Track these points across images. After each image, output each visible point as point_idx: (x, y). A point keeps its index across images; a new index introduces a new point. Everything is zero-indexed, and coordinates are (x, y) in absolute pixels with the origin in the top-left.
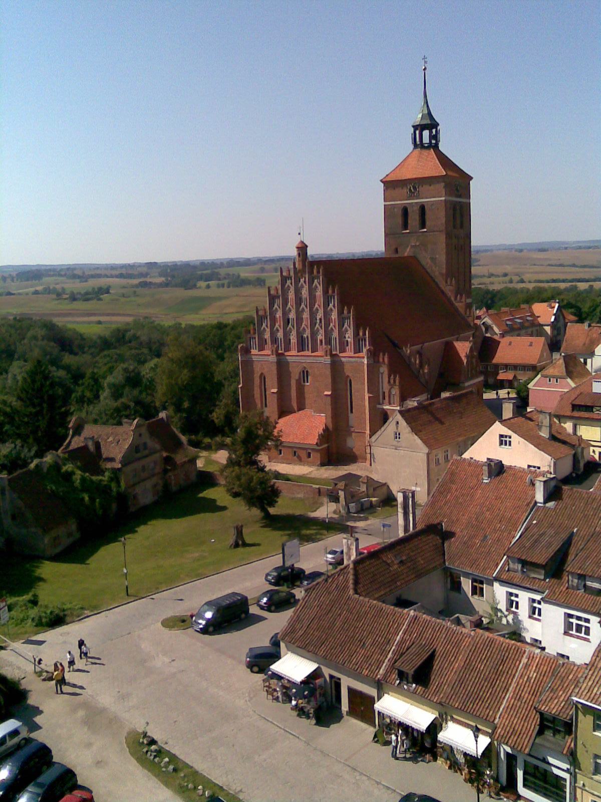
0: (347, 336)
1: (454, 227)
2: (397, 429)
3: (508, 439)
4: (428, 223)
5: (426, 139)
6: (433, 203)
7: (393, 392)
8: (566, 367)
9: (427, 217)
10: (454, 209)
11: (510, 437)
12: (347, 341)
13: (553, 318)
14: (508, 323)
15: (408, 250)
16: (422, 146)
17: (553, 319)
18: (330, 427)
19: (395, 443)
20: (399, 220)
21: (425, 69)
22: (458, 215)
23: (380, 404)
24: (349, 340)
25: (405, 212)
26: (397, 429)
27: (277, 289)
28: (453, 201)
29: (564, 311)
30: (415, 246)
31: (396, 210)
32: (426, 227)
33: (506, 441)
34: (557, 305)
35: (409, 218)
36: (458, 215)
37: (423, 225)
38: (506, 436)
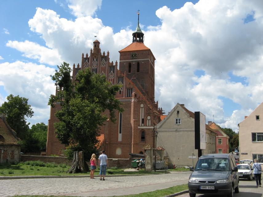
2: (178, 116)
4: (141, 69)
6: (143, 61)
12: (120, 91)
16: (137, 41)
20: (127, 69)
21: (139, 15)
23: (139, 126)
24: (121, 90)
25: (130, 65)
26: (178, 116)
27: (78, 66)
31: (125, 64)
32: (140, 71)
35: (132, 67)
36: (152, 70)
37: (138, 71)
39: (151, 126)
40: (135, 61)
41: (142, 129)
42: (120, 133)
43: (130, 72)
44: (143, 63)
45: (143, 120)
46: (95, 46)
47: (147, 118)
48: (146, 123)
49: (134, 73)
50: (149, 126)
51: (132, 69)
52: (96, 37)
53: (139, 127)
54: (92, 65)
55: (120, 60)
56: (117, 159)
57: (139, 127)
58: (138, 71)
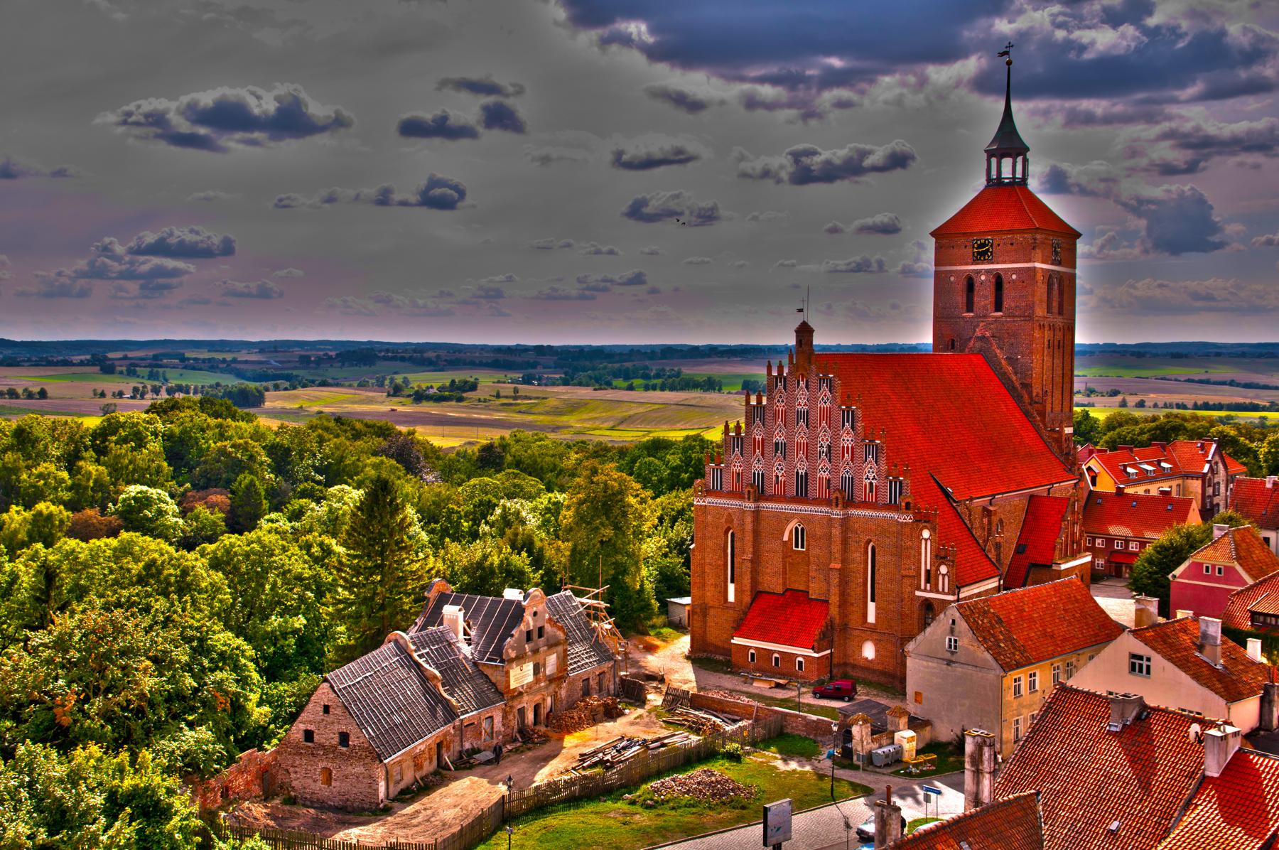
0: (871, 476)
1: (1049, 310)
3: (1145, 663)
4: (1007, 303)
5: (1006, 173)
7: (944, 569)
8: (1236, 549)
9: (1005, 292)
10: (1050, 286)
11: (1149, 660)
12: (871, 484)
13: (1207, 467)
14: (1130, 470)
15: (971, 344)
17: (1206, 470)
18: (837, 621)
19: (948, 655)
20: (961, 299)
21: (1009, 63)
22: (1056, 292)
23: (919, 589)
28: (1048, 270)
29: (1228, 460)
30: (983, 338)
33: (1141, 666)
34: (1214, 446)
38: (1141, 658)
39: (948, 594)
40: (988, 271)
41: (927, 599)
42: (873, 600)
43: (972, 311)
44: (1014, 277)
45: (928, 572)
46: (799, 342)
47: (938, 569)
48: (937, 584)
49: (985, 316)
50: (943, 592)
51: (976, 299)
52: (801, 310)
53: (918, 593)
54: (792, 399)
55: (936, 265)
56: (814, 717)
57: (918, 593)
58: (998, 307)
